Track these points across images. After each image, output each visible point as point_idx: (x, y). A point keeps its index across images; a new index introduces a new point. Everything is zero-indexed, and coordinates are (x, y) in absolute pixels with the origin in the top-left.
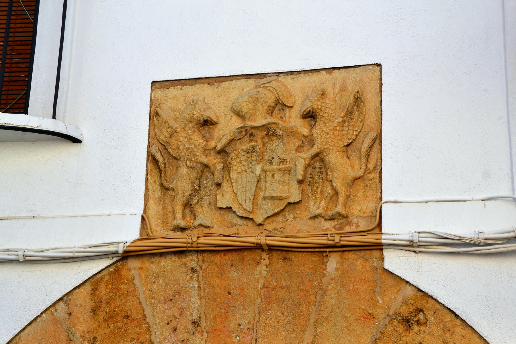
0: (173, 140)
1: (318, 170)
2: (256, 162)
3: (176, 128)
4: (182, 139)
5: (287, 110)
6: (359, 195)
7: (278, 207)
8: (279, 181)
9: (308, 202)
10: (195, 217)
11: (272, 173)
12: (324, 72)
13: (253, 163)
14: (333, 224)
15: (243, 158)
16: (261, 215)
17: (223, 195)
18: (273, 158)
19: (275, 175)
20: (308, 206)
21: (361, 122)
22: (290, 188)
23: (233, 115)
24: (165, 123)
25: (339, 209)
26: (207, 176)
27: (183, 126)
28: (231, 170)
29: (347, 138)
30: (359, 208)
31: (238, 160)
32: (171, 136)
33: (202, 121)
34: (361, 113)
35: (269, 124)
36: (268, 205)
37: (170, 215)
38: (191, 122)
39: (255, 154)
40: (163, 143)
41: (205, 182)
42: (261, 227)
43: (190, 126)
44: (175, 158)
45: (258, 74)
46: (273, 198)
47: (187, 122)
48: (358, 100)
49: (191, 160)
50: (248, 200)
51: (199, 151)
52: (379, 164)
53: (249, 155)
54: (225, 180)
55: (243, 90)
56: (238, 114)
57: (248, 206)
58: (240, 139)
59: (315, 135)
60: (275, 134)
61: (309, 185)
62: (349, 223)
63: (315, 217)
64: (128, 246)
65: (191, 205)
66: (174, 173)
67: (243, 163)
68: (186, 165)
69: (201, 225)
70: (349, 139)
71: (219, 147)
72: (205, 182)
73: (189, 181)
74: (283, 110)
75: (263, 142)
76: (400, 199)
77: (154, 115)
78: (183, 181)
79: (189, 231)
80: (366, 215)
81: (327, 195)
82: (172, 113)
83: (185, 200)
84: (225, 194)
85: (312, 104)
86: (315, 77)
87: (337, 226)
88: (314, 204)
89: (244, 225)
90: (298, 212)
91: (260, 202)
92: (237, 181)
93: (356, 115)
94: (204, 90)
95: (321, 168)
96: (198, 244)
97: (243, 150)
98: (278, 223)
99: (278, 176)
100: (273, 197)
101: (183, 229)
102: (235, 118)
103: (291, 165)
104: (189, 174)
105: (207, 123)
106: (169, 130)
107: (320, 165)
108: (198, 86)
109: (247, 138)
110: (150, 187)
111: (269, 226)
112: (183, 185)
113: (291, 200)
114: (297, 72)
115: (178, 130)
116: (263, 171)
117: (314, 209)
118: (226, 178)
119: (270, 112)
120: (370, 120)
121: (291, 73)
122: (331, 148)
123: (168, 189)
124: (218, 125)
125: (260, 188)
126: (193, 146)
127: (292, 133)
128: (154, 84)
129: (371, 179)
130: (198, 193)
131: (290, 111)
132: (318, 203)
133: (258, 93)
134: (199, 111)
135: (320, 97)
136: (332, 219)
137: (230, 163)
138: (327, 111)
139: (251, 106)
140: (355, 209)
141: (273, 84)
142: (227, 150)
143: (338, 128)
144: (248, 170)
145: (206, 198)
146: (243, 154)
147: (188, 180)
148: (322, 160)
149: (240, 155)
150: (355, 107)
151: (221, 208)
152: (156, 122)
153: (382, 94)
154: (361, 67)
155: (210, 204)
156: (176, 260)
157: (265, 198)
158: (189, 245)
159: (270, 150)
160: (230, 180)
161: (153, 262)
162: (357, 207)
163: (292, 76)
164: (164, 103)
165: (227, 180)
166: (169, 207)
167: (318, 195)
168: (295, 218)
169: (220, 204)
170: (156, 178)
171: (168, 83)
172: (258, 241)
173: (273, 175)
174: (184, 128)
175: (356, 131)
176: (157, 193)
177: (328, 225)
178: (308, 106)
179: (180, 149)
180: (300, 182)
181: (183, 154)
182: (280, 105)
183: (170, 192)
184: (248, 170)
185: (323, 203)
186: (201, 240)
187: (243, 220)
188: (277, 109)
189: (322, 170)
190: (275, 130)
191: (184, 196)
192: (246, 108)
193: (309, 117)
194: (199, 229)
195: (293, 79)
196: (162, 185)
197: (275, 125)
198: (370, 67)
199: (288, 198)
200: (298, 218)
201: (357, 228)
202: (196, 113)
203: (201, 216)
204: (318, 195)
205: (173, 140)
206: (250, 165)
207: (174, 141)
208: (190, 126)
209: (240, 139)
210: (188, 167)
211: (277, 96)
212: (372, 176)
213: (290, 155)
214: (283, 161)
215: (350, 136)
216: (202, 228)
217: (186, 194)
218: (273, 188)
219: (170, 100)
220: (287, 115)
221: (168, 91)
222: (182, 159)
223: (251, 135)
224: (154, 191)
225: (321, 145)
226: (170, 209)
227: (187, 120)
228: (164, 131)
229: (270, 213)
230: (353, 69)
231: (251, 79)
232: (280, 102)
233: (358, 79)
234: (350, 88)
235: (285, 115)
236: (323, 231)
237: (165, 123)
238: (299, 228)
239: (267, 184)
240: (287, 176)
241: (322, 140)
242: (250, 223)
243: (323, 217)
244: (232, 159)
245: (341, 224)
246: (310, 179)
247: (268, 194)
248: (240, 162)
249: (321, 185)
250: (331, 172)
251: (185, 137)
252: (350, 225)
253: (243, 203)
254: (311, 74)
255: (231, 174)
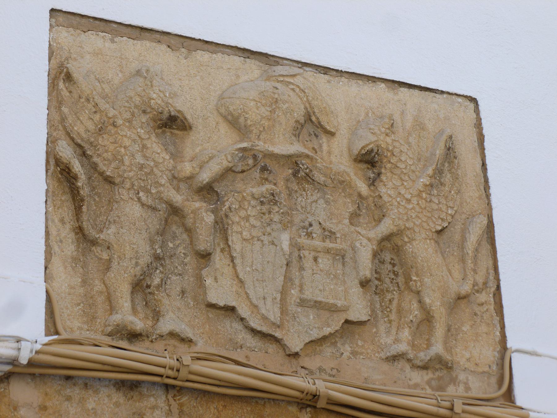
0: (104, 141)
1: (390, 267)
2: (279, 226)
3: (114, 116)
4: (127, 142)
5: (324, 139)
6: (464, 328)
7: (329, 326)
8: (328, 274)
9: (376, 326)
10: (157, 315)
11: (313, 254)
12: (383, 85)
13: (274, 226)
14: (426, 378)
15: (252, 212)
16: (296, 335)
17: (216, 279)
18: (311, 225)
19: (320, 260)
20: (376, 333)
21: (457, 194)
22: (346, 291)
23: (220, 120)
24: (88, 100)
25: (438, 348)
26: (175, 233)
27: (127, 115)
28: (230, 231)
29: (439, 217)
30: (468, 355)
31: (242, 213)
32: (101, 131)
33: (165, 116)
34: (456, 178)
35: (300, 155)
36: (307, 316)
37: (100, 299)
38: (144, 112)
39: (276, 209)
40: (79, 141)
41: (171, 245)
42: (294, 361)
43: (144, 120)
44: (109, 180)
45: (266, 55)
46: (318, 305)
47: (136, 111)
48: (450, 152)
49: (148, 191)
50: (269, 301)
51: (165, 177)
52: (491, 277)
53: (265, 208)
54: (218, 250)
55: (238, 77)
56: (234, 122)
57: (274, 314)
58: (243, 172)
59: (386, 198)
60: (308, 178)
61: (376, 293)
62: (454, 381)
63: (394, 358)
64: (37, 352)
65: (148, 287)
66: (103, 210)
67: (252, 221)
68: (139, 199)
69: (172, 335)
70: (443, 220)
71: (205, 177)
72: (171, 245)
73: (145, 235)
74: (317, 136)
75: (287, 188)
76: (540, 350)
77: (61, 76)
78: (130, 230)
79: (147, 343)
80: (480, 370)
81: (411, 318)
82: (98, 84)
83: (138, 274)
84: (219, 277)
85: (376, 139)
86: (367, 89)
87: (434, 383)
88: (388, 332)
89: (260, 350)
90: (360, 343)
91: (292, 308)
92: (243, 257)
93: (447, 178)
94: (159, 58)
95: (394, 265)
96: (190, 373)
97: (253, 196)
98: (324, 359)
99: (324, 262)
100: (320, 302)
101: (134, 336)
102: (224, 128)
103: (344, 246)
104: (145, 221)
105: (172, 124)
106: (97, 117)
107: (392, 259)
108: (148, 43)
109: (256, 174)
110: (53, 231)
111: (312, 363)
112: (135, 241)
113: (353, 316)
114: (337, 71)
115: (120, 122)
116: (296, 246)
117: (389, 341)
118: (219, 245)
119: (297, 132)
120: (471, 193)
121: (326, 70)
122: (417, 229)
123: (94, 243)
124: (192, 133)
125: (291, 280)
126: (152, 164)
127: (342, 184)
128: (54, 14)
129: (482, 304)
130: (162, 265)
131: (328, 141)
132: (394, 331)
133: (276, 91)
134: (162, 95)
135: (389, 128)
136: (425, 368)
137: (227, 216)
138: (403, 159)
139: (265, 111)
140: (461, 356)
141: (298, 80)
142: (218, 188)
143: (424, 195)
144: (265, 239)
145: (174, 278)
146: (253, 202)
147: (144, 232)
148: (397, 250)
149: (246, 203)
150: (447, 165)
151: (212, 306)
152: (65, 93)
153: (486, 152)
154: (445, 96)
155: (183, 292)
156: (122, 400)
157: (302, 303)
158: (170, 373)
159: (302, 207)
160: (227, 248)
161: (69, 399)
162: (464, 352)
163: (326, 77)
164: (75, 59)
165: (222, 250)
166: (97, 282)
167: (393, 316)
168: (354, 353)
169: (213, 297)
170: (67, 212)
171: (84, 20)
172: (312, 388)
173: (315, 259)
174: (130, 121)
175: (452, 208)
176: (70, 248)
177: (417, 377)
178: (365, 140)
179: (122, 161)
180: (364, 284)
181: (131, 174)
182: (312, 125)
183: (97, 250)
184: (265, 239)
185: (406, 334)
186: (199, 367)
187: (257, 338)
188: (305, 131)
189: (396, 269)
190: (311, 171)
191: (137, 264)
192: (255, 114)
193: (367, 162)
194: (167, 342)
195: (329, 82)
196: (80, 231)
197: (309, 161)
198: (460, 100)
199: (345, 309)
200: (361, 354)
201: (467, 392)
202: (155, 96)
203: (171, 314)
204: (393, 316)
205: (104, 141)
206: (268, 229)
207: (106, 143)
208: (144, 120)
209: (243, 172)
210: (143, 205)
211: (308, 106)
212: (482, 297)
213: (340, 226)
214: (330, 235)
215: (443, 216)
216: (173, 342)
217: (141, 262)
218: (319, 282)
219: (88, 57)
220: (325, 147)
221: (83, 36)
222: (128, 185)
223: (264, 169)
224: (61, 241)
225: (399, 219)
226: (98, 286)
227: (136, 106)
228: (84, 117)
229: (315, 334)
230: (432, 94)
231: (253, 61)
232: (314, 119)
233: (442, 116)
234: (430, 126)
235: (321, 146)
236: (409, 387)
237: (88, 100)
238: (366, 375)
239: (304, 273)
240: (340, 266)
241: (401, 210)
242: (272, 348)
243: (409, 360)
244: (230, 208)
245: (440, 378)
246: (377, 282)
247: (308, 294)
248: (247, 218)
249: (396, 297)
250: (417, 275)
251: (134, 141)
252: (455, 384)
253: (261, 304)
254: (360, 82)
255: (230, 239)
